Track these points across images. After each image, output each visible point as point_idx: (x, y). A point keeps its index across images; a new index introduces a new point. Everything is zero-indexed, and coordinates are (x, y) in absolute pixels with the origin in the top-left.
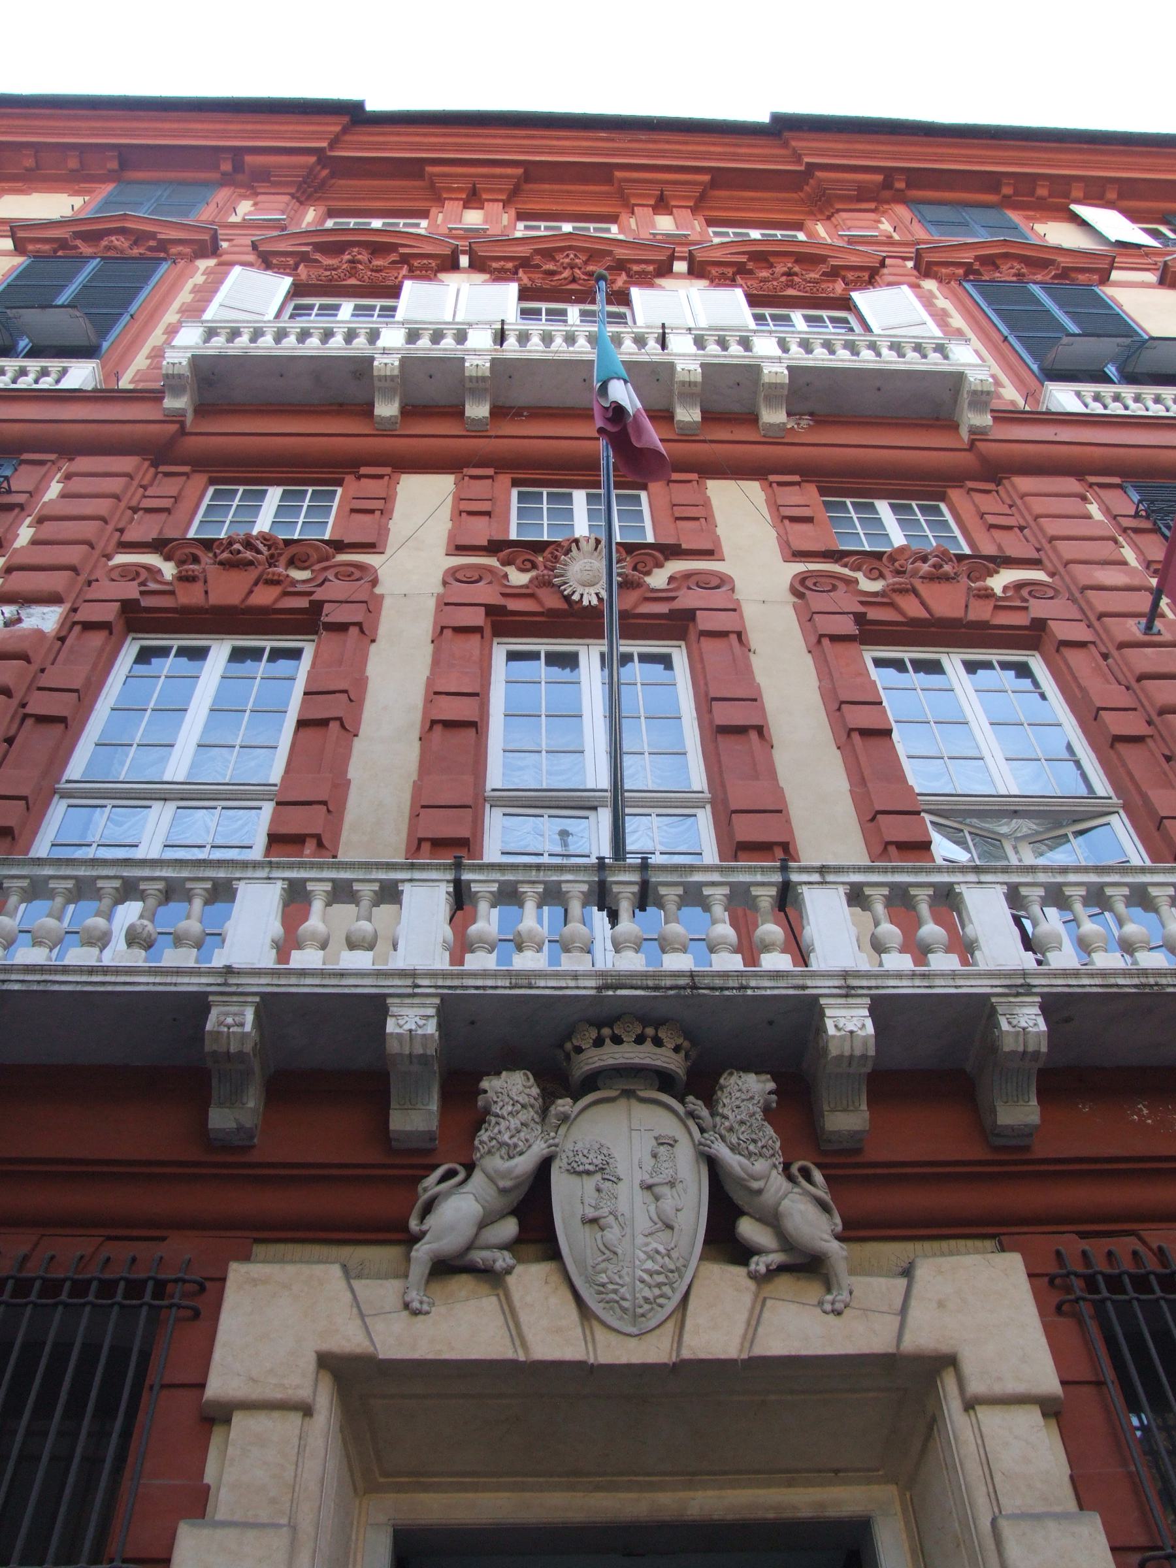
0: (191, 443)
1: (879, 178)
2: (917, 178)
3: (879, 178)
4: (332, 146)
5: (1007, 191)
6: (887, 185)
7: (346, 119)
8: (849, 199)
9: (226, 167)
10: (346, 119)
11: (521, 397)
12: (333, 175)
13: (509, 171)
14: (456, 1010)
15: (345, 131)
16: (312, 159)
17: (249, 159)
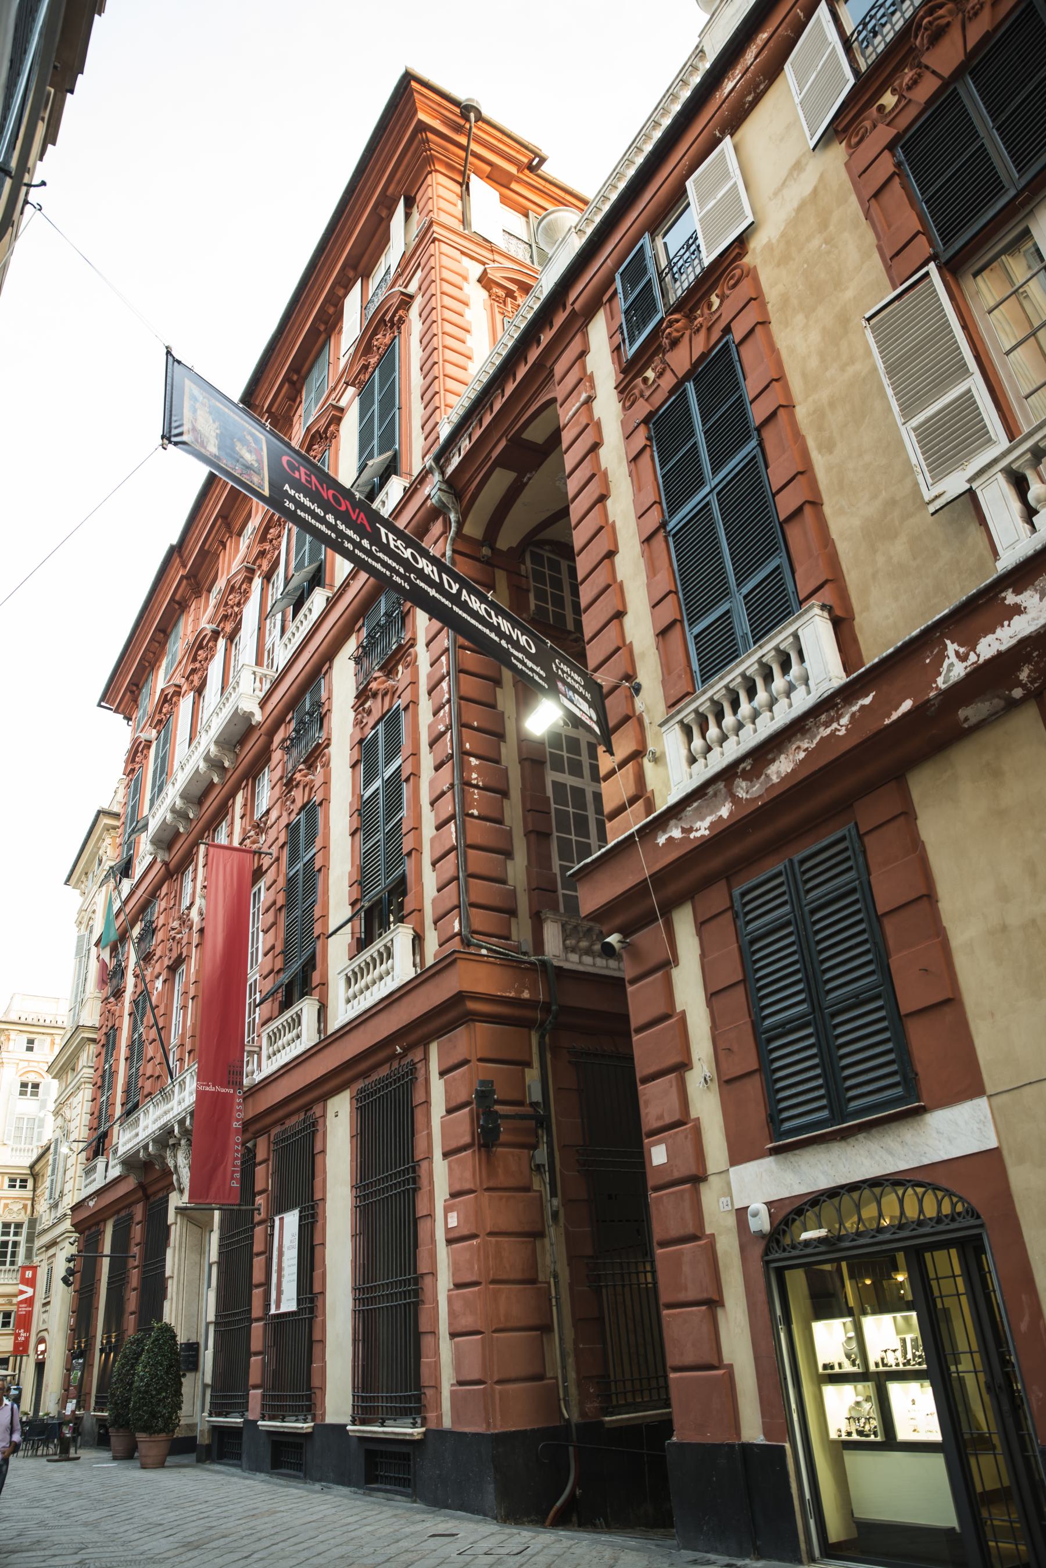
0: (172, 865)
1: (287, 385)
2: (295, 368)
3: (287, 385)
4: (185, 567)
5: (322, 328)
6: (293, 384)
7: (176, 554)
8: (290, 408)
9: (177, 607)
10: (176, 554)
11: (197, 791)
12: (195, 577)
13: (218, 523)
14: (154, 1141)
15: (181, 557)
16: (185, 582)
17: (177, 598)
